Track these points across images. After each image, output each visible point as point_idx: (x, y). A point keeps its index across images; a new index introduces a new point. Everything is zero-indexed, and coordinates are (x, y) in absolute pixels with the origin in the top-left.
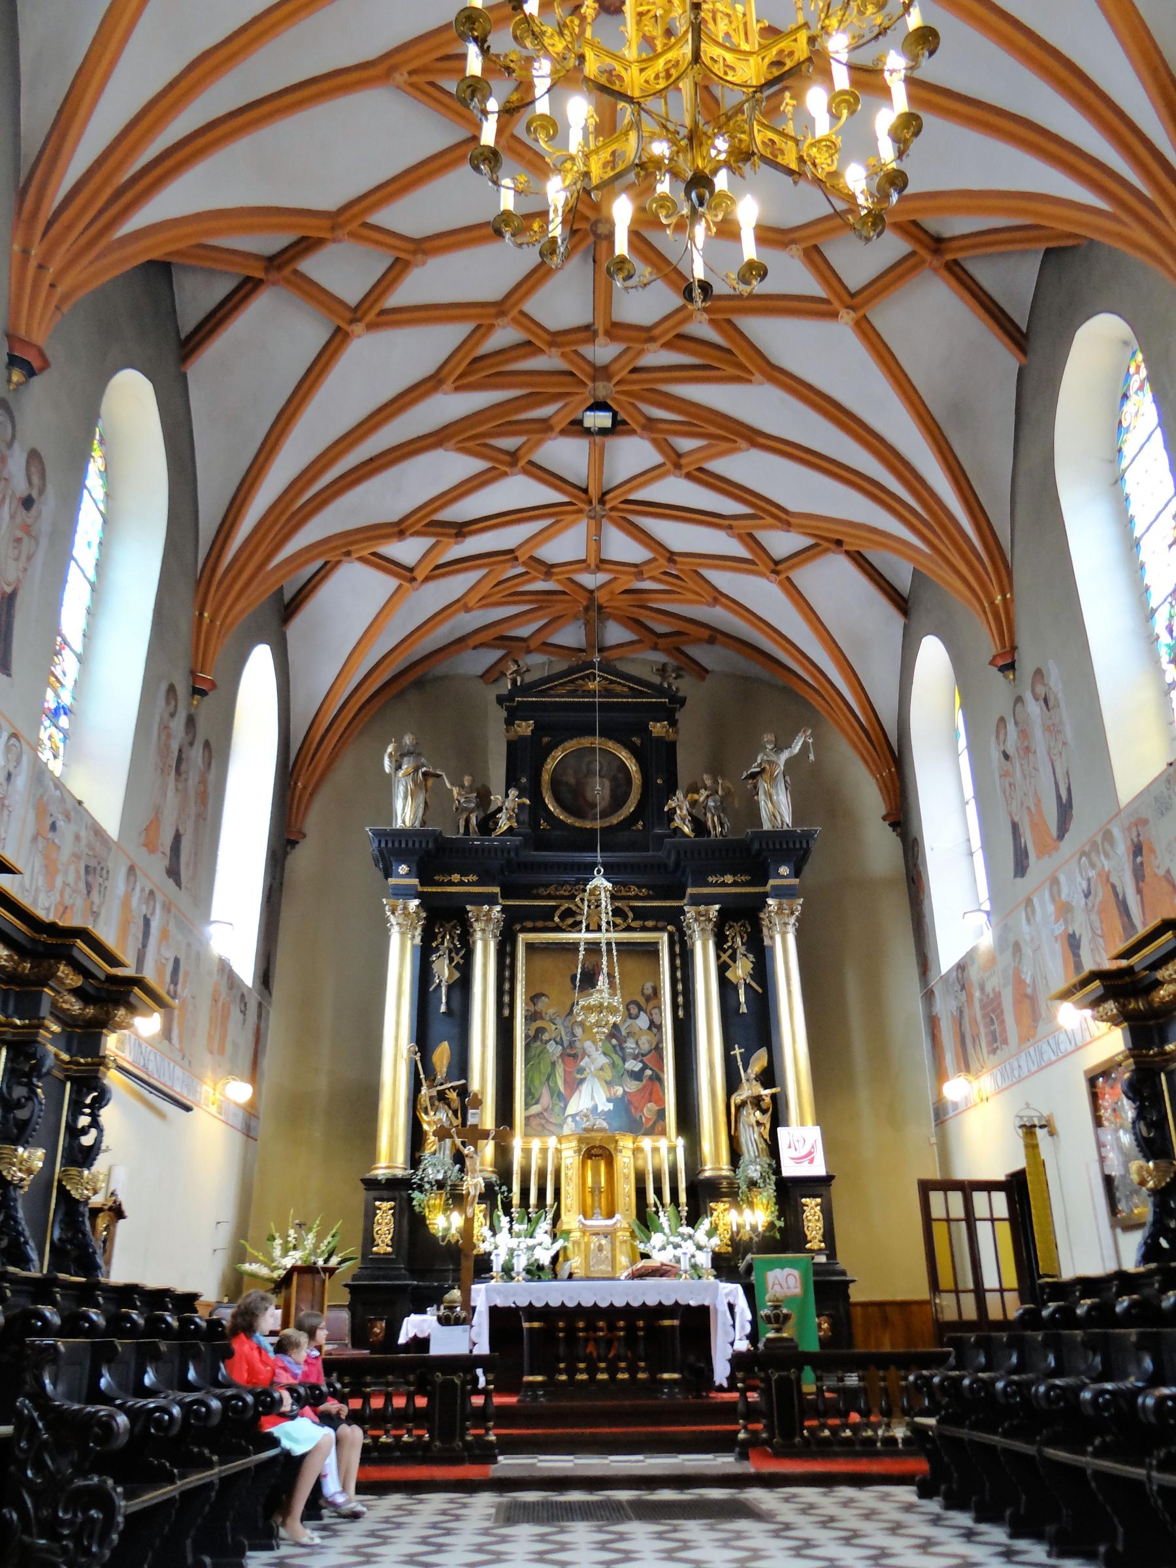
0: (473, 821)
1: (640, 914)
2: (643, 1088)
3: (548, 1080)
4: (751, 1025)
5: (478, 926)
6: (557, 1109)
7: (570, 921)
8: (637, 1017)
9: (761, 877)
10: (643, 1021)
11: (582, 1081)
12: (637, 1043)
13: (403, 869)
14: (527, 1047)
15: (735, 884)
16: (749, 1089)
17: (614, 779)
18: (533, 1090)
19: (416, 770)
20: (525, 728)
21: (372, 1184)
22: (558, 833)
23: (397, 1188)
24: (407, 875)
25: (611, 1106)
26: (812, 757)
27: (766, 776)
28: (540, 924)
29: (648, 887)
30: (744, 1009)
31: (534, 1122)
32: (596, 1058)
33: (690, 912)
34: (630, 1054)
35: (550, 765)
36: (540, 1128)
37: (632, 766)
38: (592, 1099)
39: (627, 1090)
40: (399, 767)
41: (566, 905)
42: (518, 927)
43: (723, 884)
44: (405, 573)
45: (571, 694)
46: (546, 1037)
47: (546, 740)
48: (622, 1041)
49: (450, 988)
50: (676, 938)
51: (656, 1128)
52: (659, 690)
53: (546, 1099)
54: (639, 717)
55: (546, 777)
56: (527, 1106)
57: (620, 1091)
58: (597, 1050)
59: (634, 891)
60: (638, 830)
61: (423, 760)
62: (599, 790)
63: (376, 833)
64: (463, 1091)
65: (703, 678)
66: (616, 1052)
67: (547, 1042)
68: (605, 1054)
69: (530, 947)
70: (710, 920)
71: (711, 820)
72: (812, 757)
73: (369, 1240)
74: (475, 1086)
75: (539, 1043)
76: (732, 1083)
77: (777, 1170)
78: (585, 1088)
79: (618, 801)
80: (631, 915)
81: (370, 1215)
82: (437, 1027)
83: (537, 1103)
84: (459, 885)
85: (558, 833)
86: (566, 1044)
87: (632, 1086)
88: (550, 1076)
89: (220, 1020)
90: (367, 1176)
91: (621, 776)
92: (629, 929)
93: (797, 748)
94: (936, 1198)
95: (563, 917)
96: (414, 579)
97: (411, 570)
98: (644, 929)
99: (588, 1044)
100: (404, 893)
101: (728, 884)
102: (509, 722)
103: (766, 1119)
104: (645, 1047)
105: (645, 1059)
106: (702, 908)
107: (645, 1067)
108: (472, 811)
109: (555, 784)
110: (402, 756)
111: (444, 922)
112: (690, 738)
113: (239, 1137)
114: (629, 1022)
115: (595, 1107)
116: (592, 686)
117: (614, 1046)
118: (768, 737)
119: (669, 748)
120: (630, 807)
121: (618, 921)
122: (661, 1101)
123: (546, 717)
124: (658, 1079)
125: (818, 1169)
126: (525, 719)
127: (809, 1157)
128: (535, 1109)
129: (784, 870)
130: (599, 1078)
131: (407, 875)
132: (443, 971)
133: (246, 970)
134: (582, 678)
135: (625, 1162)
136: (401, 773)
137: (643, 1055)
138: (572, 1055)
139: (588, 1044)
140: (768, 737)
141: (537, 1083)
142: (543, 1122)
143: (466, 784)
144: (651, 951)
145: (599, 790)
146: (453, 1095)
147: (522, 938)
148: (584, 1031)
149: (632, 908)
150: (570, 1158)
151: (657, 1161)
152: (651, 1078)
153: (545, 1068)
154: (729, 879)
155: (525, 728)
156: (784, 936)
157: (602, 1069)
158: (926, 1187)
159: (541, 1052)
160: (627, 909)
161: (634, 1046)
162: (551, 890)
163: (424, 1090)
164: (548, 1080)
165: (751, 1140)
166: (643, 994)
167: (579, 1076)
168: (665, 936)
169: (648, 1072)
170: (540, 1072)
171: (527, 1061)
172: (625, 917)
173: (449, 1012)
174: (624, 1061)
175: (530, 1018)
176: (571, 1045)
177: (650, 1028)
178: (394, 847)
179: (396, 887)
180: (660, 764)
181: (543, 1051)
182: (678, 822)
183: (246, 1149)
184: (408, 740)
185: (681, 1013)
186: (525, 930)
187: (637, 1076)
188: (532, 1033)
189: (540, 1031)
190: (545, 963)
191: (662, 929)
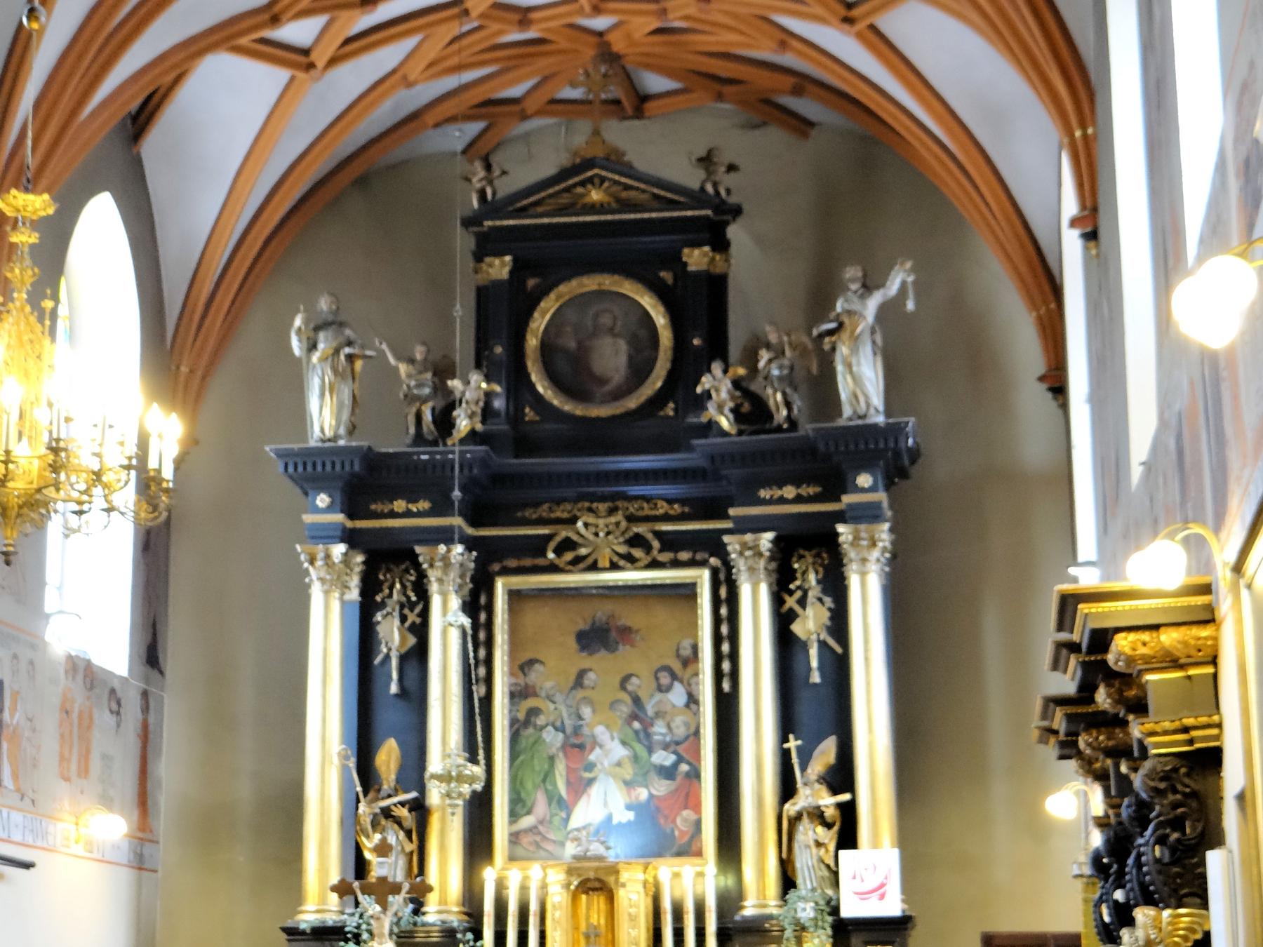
0: (428, 416)
1: (671, 542)
2: (676, 790)
3: (544, 781)
4: (811, 703)
5: (433, 575)
6: (556, 820)
7: (569, 556)
8: (668, 689)
9: (835, 484)
10: (677, 696)
11: (591, 782)
12: (669, 727)
13: (322, 500)
14: (514, 738)
15: (799, 499)
17: (633, 341)
18: (523, 795)
19: (337, 351)
20: (500, 268)
22: (550, 426)
24: (329, 509)
25: (631, 816)
26: (910, 305)
27: (845, 335)
28: (528, 562)
29: (683, 502)
30: (816, 678)
31: (526, 840)
32: (611, 750)
33: (732, 543)
34: (659, 742)
35: (539, 322)
36: (531, 848)
37: (661, 320)
38: (605, 805)
39: (654, 792)
40: (313, 347)
41: (564, 533)
42: (496, 567)
43: (782, 501)
44: (299, 58)
45: (561, 211)
46: (541, 720)
47: (531, 283)
48: (647, 725)
49: (403, 659)
50: (722, 576)
51: (689, 849)
52: (698, 198)
53: (541, 806)
54: (670, 243)
55: (532, 342)
56: (514, 816)
57: (643, 794)
58: (613, 738)
59: (663, 508)
60: (668, 417)
61: (348, 332)
62: (611, 358)
63: (281, 454)
64: (420, 808)
65: (805, 135)
66: (639, 741)
67: (542, 728)
68: (624, 743)
69: (515, 596)
70: (760, 555)
71: (775, 398)
72: (910, 305)
75: (530, 730)
76: (787, 789)
77: (835, 911)
78: (595, 791)
79: (639, 372)
80: (656, 544)
82: (388, 714)
83: (529, 813)
84: (403, 516)
85: (550, 426)
86: (569, 730)
87: (661, 787)
88: (548, 776)
89: (77, 731)
90: (289, 923)
91: (643, 333)
92: (654, 565)
93: (893, 287)
95: (559, 551)
96: (311, 66)
97: (306, 52)
98: (676, 564)
99: (600, 730)
100: (323, 535)
101: (787, 500)
102: (479, 256)
103: (829, 837)
104: (680, 731)
105: (680, 749)
106: (749, 537)
107: (680, 759)
108: (424, 400)
109: (548, 350)
110: (317, 329)
111: (387, 567)
112: (754, 267)
113: (125, 876)
114: (658, 696)
115: (609, 818)
116: (595, 195)
117: (636, 732)
118: (852, 273)
119: (716, 285)
120: (656, 381)
121: (637, 553)
122: (697, 808)
123: (536, 247)
124: (695, 775)
125: (892, 907)
126: (500, 254)
127: (880, 890)
128: (526, 822)
129: (864, 480)
130: (614, 777)
131: (329, 509)
133: (114, 653)
134: (582, 184)
135: (632, 898)
136: (315, 358)
137: (677, 743)
138: (577, 745)
139: (600, 730)
141: (529, 785)
142: (538, 838)
143: (419, 357)
144: (687, 592)
145: (611, 358)
146: (404, 812)
147: (500, 586)
148: (594, 711)
149: (659, 535)
150: (558, 897)
151: (677, 894)
152: (688, 775)
153: (539, 765)
154: (789, 492)
155: (500, 268)
156: (863, 574)
157: (619, 764)
159: (536, 742)
160: (650, 536)
161: (664, 730)
162: (543, 511)
163: (362, 808)
164: (544, 781)
165: (806, 863)
166: (678, 656)
167: (587, 775)
168: (706, 574)
169: (684, 767)
170: (533, 770)
171: (514, 754)
172: (648, 548)
173: (403, 693)
174: (650, 751)
175: (516, 695)
176: (577, 730)
177: (687, 706)
178: (310, 468)
179: (314, 526)
180: (703, 313)
181: (538, 741)
182: (712, 410)
183: (139, 885)
184: (324, 304)
185: (726, 686)
186: (506, 572)
187: (668, 773)
188: (521, 716)
189: (534, 712)
190: (535, 616)
191: (703, 564)
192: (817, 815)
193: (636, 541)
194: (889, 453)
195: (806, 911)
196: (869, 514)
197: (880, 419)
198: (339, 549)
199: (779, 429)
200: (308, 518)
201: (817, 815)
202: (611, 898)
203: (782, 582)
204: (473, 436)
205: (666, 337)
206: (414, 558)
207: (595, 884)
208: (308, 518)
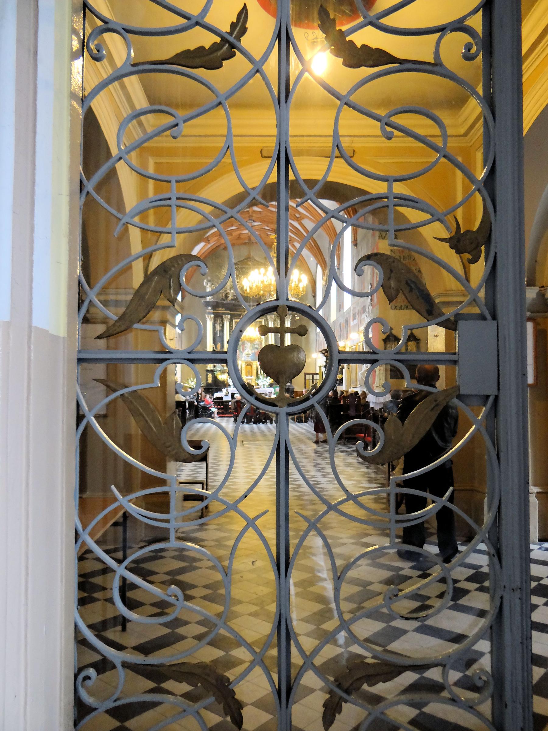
13: (210, 308)
21: (207, 371)
57: (253, 351)
69: (236, 322)
73: (207, 380)
81: (207, 376)
84: (221, 310)
94: (307, 376)
100: (209, 313)
111: (218, 317)
132: (218, 328)
136: (208, 286)
147: (234, 321)
158: (305, 374)
168: (264, 320)
173: (220, 336)
200: (208, 311)
202: (251, 366)
204: (232, 300)
208: (208, 311)
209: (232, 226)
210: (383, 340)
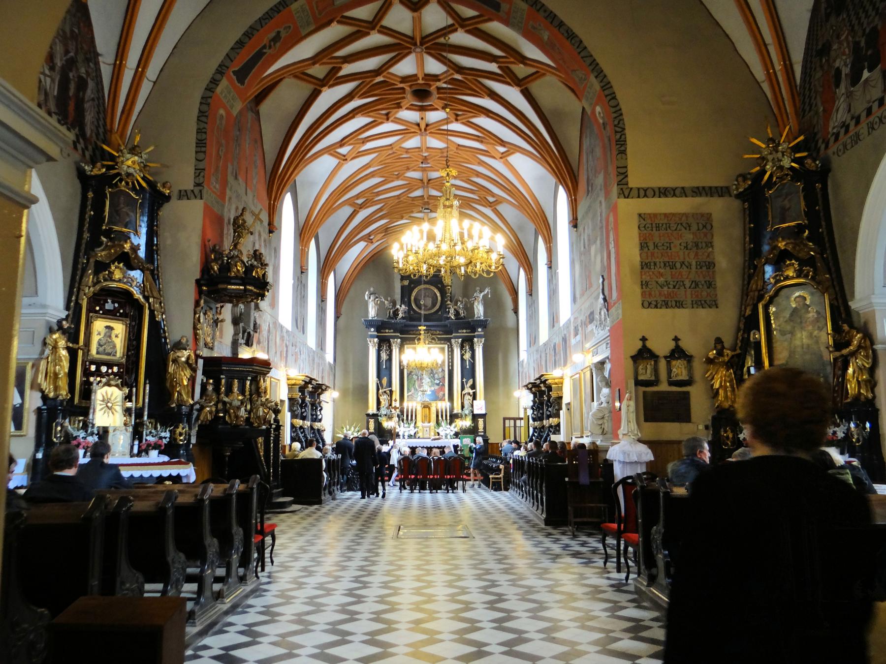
4: (469, 372)
9: (474, 330)
13: (372, 329)
16: (468, 390)
20: (406, 283)
21: (368, 415)
23: (375, 416)
33: (453, 341)
35: (414, 294)
37: (438, 295)
51: (443, 399)
53: (413, 390)
55: (412, 298)
64: (391, 391)
71: (461, 312)
74: (394, 389)
76: (463, 389)
79: (434, 305)
81: (368, 422)
82: (383, 372)
84: (388, 333)
87: (437, 387)
88: (414, 384)
94: (507, 421)
100: (372, 337)
101: (464, 333)
103: (471, 398)
109: (415, 299)
118: (478, 288)
124: (443, 385)
125: (483, 412)
127: (481, 408)
129: (480, 330)
132: (384, 356)
135: (433, 410)
140: (478, 288)
150: (419, 409)
155: (406, 283)
158: (505, 419)
165: (467, 403)
178: (370, 324)
184: (372, 289)
187: (438, 384)
192: (469, 394)
193: (433, 339)
194: (483, 324)
195: (467, 412)
196: (479, 336)
197: (482, 318)
198: (376, 340)
199: (461, 318)
201: (469, 394)
202: (429, 409)
203: (462, 347)
205: (439, 298)
206: (389, 342)
207: (426, 406)
209: (402, 218)
210: (632, 357)
